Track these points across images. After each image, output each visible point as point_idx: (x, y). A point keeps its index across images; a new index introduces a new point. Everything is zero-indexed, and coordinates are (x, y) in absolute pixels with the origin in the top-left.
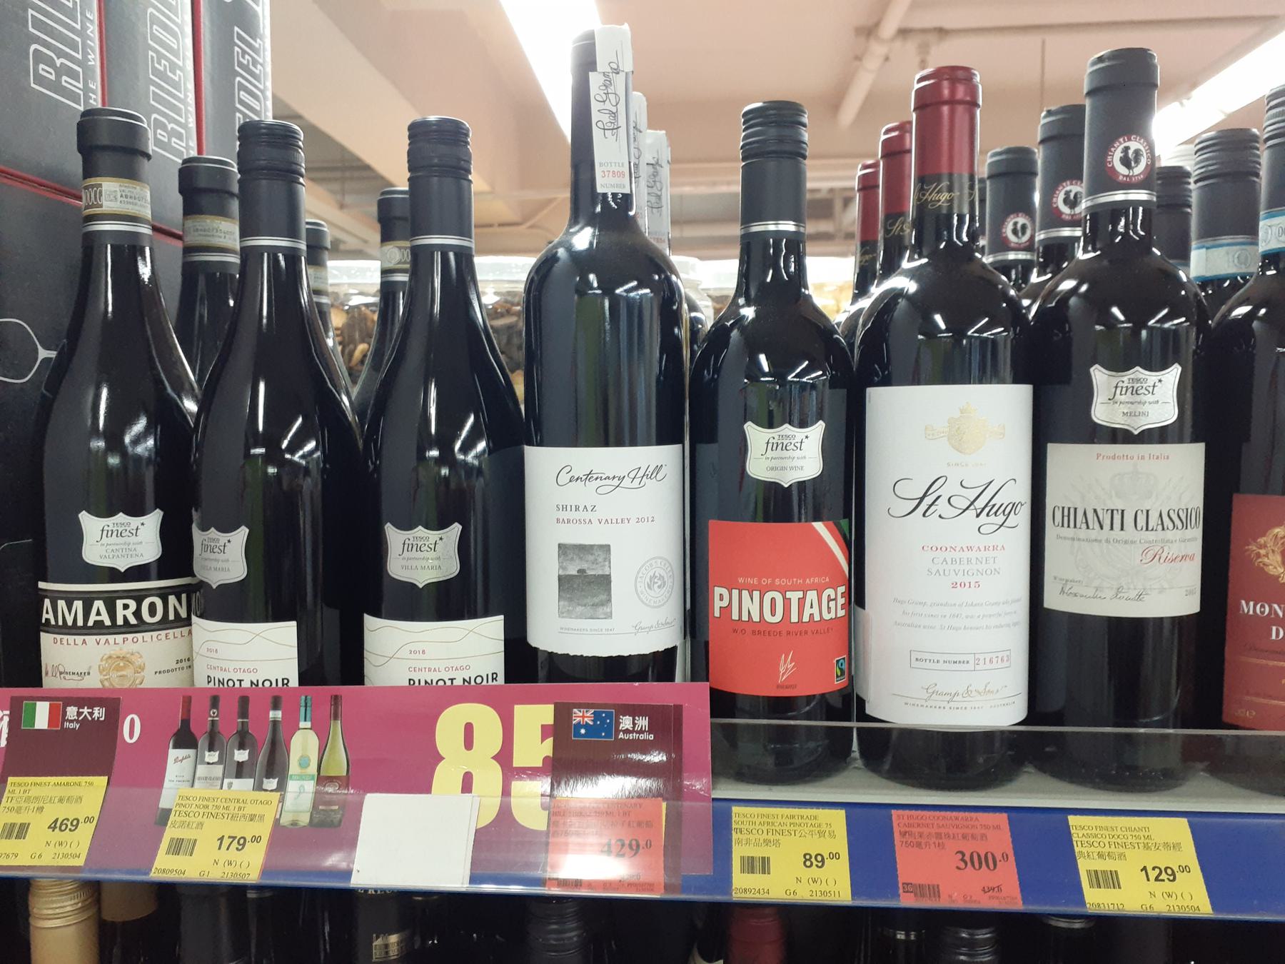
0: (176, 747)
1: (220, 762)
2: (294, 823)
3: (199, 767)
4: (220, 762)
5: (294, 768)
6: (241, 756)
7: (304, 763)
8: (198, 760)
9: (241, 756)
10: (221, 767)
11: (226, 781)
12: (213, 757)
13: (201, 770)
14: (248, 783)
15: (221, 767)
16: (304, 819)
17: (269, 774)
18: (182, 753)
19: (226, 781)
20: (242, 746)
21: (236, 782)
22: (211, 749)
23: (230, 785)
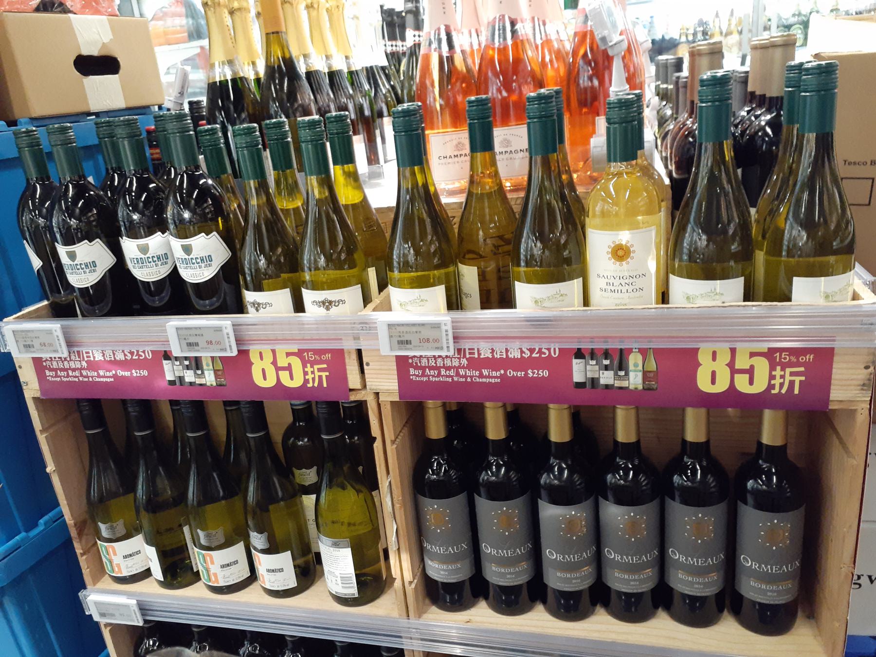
0: (576, 358)
1: (597, 364)
2: (636, 389)
3: (588, 367)
4: (597, 364)
5: (631, 367)
6: (607, 362)
7: (636, 365)
8: (586, 364)
9: (607, 362)
10: (597, 367)
11: (601, 372)
12: (594, 362)
13: (588, 367)
14: (612, 373)
15: (597, 367)
16: (640, 387)
17: (620, 369)
18: (578, 361)
19: (601, 372)
20: (606, 358)
21: (606, 372)
22: (592, 359)
23: (603, 373)
